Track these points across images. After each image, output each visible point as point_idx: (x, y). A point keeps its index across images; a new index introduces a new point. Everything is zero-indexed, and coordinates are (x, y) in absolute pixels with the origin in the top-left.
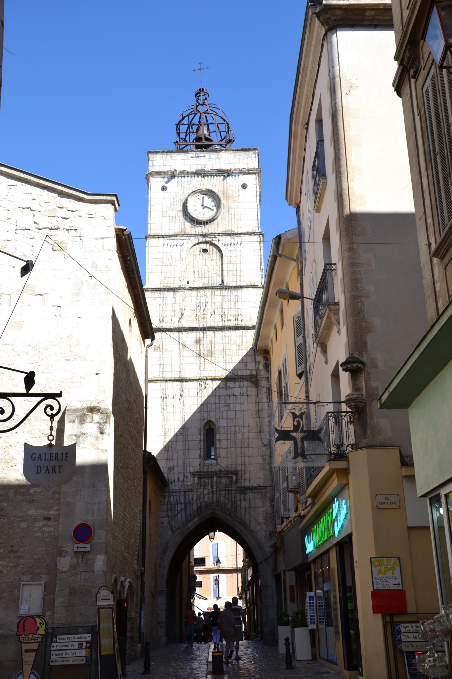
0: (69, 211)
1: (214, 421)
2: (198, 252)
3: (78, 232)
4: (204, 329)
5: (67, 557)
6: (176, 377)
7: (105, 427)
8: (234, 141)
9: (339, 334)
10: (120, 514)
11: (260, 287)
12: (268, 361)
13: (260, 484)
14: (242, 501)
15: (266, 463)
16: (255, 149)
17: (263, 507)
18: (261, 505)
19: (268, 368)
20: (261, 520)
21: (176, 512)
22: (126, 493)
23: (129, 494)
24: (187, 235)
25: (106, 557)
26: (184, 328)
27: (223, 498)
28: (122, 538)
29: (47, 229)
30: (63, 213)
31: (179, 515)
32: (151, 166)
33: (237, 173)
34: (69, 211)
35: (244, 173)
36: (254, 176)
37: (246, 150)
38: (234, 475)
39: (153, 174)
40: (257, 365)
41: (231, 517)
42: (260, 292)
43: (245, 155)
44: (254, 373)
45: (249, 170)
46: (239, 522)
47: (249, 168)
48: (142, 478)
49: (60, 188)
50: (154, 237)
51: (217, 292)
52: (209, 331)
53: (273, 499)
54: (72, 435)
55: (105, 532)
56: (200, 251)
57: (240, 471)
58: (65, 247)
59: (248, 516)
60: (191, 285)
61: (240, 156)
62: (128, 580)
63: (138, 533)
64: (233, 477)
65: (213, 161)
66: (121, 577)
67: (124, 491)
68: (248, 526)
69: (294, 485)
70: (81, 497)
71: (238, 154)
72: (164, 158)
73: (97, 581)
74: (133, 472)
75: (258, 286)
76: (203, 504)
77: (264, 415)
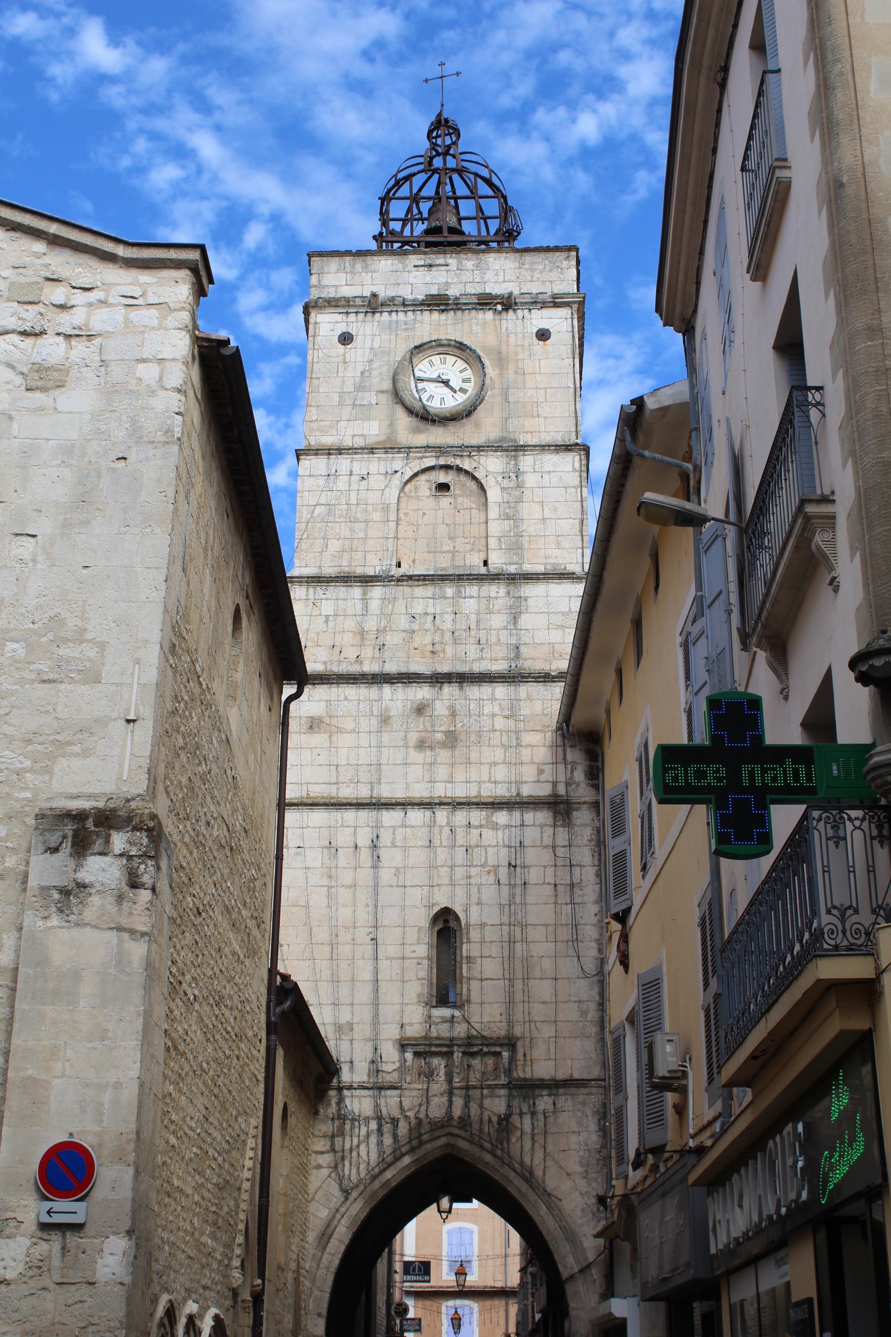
0: (74, 288)
1: (458, 910)
2: (427, 493)
3: (97, 341)
4: (438, 679)
5: (19, 1238)
6: (363, 796)
7: (143, 867)
8: (519, 233)
9: (836, 590)
10: (191, 1129)
11: (578, 578)
12: (596, 760)
13: (572, 1074)
14: (524, 1116)
15: (589, 1019)
16: (569, 249)
17: (579, 1133)
19: (598, 778)
22: (212, 1072)
23: (222, 1077)
24: (399, 450)
25: (133, 1243)
26: (388, 674)
28: (196, 1196)
29: (15, 338)
30: (59, 294)
31: (363, 1148)
32: (315, 286)
33: (526, 303)
34: (74, 288)
35: (544, 303)
36: (565, 312)
38: (506, 1048)
40: (569, 772)
41: (495, 1156)
42: (579, 589)
43: (547, 262)
44: (561, 790)
45: (554, 296)
46: (514, 1170)
47: (556, 291)
48: (264, 1041)
49: (53, 228)
50: (317, 452)
51: (472, 590)
52: (449, 682)
53: (605, 1113)
54: (48, 888)
55: (131, 1170)
56: (430, 489)
58: (60, 381)
59: (539, 1154)
60: (404, 570)
61: (532, 264)
62: (213, 1311)
63: (246, 1185)
64: (504, 1053)
65: (467, 276)
66: (190, 1302)
67: (205, 1065)
68: (540, 1181)
69: (670, 1068)
70: (67, 1065)
71: (528, 258)
72: (348, 269)
73: (105, 1313)
74: (235, 1018)
75: (574, 573)
77: (586, 898)
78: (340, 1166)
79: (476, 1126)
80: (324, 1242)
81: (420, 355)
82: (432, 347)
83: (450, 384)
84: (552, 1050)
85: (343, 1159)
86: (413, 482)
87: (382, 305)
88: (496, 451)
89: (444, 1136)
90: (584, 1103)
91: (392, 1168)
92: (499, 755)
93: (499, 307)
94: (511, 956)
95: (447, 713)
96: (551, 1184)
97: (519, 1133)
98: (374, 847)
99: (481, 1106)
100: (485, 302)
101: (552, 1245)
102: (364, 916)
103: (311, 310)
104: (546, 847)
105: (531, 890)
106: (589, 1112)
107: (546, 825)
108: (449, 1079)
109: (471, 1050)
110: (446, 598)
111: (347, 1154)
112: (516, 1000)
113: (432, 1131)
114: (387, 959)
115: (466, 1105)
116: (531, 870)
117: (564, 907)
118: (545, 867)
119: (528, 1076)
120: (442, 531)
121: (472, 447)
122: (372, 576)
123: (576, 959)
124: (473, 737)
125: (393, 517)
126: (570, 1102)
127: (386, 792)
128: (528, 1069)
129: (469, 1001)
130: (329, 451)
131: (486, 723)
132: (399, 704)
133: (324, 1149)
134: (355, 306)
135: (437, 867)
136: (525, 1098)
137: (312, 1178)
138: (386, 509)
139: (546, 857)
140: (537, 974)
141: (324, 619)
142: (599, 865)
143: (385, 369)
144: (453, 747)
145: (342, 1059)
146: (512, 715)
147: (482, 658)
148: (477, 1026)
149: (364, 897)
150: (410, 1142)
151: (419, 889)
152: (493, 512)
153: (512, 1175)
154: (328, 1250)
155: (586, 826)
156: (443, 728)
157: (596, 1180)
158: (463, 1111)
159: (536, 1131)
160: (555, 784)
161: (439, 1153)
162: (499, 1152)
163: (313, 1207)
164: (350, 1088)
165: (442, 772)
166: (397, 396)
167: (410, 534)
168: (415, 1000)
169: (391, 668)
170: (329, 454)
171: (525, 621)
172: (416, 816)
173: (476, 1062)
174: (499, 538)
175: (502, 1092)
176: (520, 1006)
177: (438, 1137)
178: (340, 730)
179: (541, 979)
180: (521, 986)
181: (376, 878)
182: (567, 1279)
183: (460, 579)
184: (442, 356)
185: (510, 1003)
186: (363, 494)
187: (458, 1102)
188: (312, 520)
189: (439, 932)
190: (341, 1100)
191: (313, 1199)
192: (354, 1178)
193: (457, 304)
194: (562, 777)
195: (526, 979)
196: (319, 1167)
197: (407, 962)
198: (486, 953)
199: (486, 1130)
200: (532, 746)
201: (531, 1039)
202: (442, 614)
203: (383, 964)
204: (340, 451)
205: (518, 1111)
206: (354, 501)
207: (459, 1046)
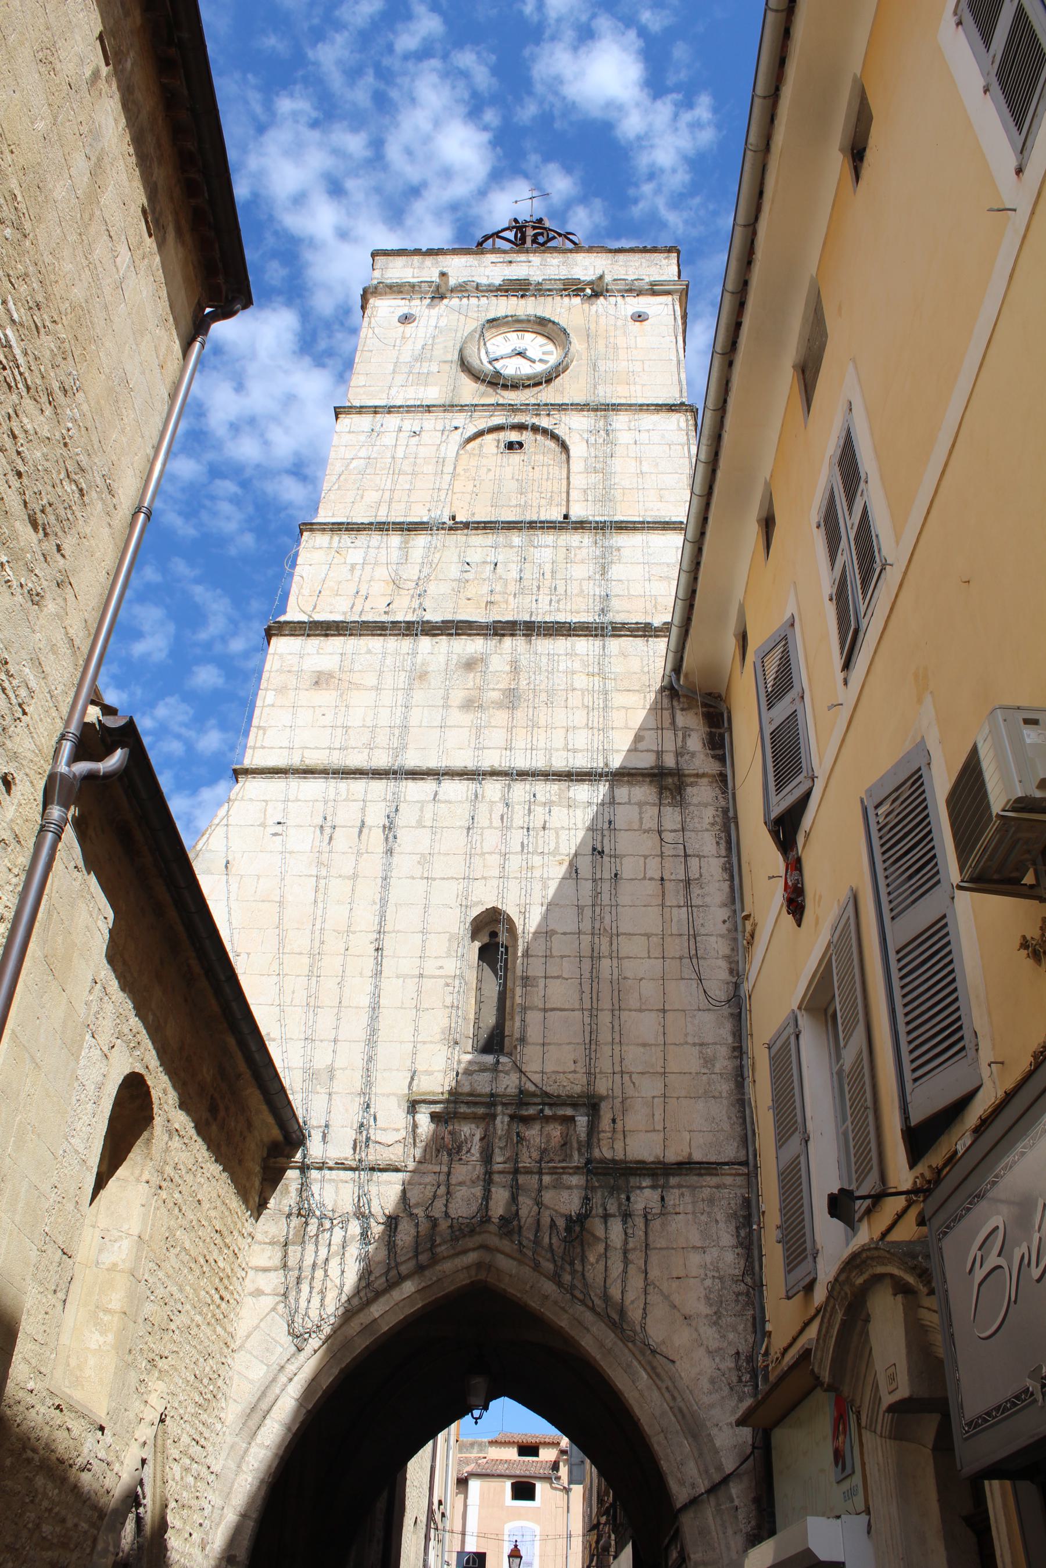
13: (690, 1154)
18: (695, 1239)
19: (722, 746)
20: (694, 1301)
21: (323, 1252)
24: (462, 408)
27: (529, 1202)
33: (619, 291)
37: (645, 250)
38: (583, 1110)
39: (379, 290)
41: (560, 1284)
44: (670, 761)
45: (653, 284)
46: (593, 1309)
50: (361, 410)
51: (548, 538)
52: (512, 635)
57: (607, 1097)
59: (636, 1282)
68: (638, 1328)
76: (444, 1225)
77: (708, 900)
80: (252, 1423)
81: (494, 330)
82: (507, 323)
83: (528, 354)
84: (658, 1117)
86: (479, 441)
87: (452, 291)
88: (582, 410)
89: (473, 1250)
90: (711, 1201)
91: (382, 1300)
92: (579, 718)
93: (589, 291)
94: (595, 977)
95: (508, 668)
96: (656, 1333)
97: (601, 1248)
98: (389, 828)
99: (539, 1203)
100: (572, 288)
101: (658, 1443)
102: (366, 918)
103: (369, 296)
104: (647, 831)
105: (625, 888)
107: (648, 803)
108: (487, 1157)
109: (524, 1113)
110: (512, 547)
111: (307, 1273)
112: (601, 1038)
113: (455, 1239)
114: (398, 977)
115: (514, 1198)
116: (625, 861)
117: (675, 911)
118: (646, 857)
119: (619, 1156)
120: (514, 485)
121: (552, 405)
123: (694, 984)
124: (544, 696)
125: (449, 469)
126: (688, 1198)
127: (412, 760)
128: (619, 1145)
129: (523, 1040)
130: (375, 410)
131: (560, 681)
132: (442, 659)
134: (421, 292)
135: (483, 854)
136: (613, 1190)
137: (244, 1312)
139: (649, 844)
140: (633, 1002)
141: (349, 567)
142: (729, 856)
143: (451, 343)
145: (313, 1122)
146: (602, 674)
147: (558, 610)
148: (536, 1078)
149: (369, 890)
150: (416, 1256)
151: (454, 883)
152: (576, 465)
153: (588, 1317)
154: (259, 1439)
155: (706, 805)
156: (501, 686)
157: (735, 1329)
159: (631, 1245)
160: (659, 754)
161: (463, 1280)
162: (567, 1278)
163: (239, 1362)
164: (321, 1167)
165: (496, 737)
166: (465, 366)
168: (438, 1037)
169: (434, 616)
170: (376, 413)
171: (616, 571)
172: (455, 789)
173: (533, 1133)
174: (585, 491)
175: (575, 1180)
176: (607, 1050)
177: (465, 1252)
178: (358, 687)
179: (640, 1010)
180: (609, 1019)
181: (388, 867)
182: (685, 1507)
183: (532, 528)
184: (520, 333)
185: (591, 1044)
186: (412, 449)
187: (500, 1197)
189: (482, 950)
190: (304, 1186)
192: (314, 1314)
193: (540, 290)
194: (669, 745)
195: (617, 1010)
196: (258, 1293)
197: (428, 984)
198: (553, 971)
199: (546, 1240)
200: (627, 709)
202: (505, 563)
203: (390, 986)
204: (390, 409)
205: (600, 1211)
206: (400, 454)
207: (504, 1104)
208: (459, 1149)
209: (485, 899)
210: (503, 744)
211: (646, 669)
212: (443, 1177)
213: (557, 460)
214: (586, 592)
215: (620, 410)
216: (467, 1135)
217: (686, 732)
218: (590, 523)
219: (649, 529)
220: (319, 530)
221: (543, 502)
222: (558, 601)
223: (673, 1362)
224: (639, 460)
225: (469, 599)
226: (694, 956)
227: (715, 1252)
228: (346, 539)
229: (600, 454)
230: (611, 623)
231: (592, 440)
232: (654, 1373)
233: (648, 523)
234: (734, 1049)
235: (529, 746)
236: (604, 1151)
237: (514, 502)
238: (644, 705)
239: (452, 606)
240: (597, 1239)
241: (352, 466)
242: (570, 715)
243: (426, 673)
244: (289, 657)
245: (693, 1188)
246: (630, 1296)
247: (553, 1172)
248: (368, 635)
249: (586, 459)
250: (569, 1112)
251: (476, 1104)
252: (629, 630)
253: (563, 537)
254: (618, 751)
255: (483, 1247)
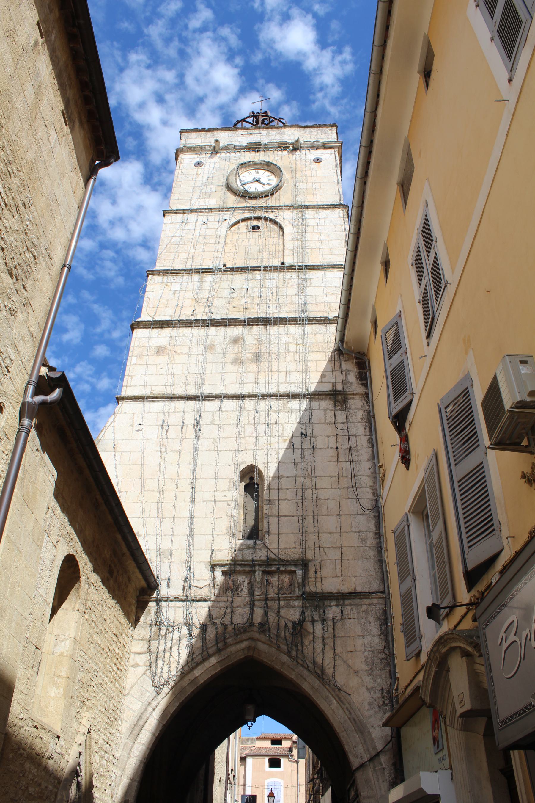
1: (261, 467)
13: (355, 588)
14: (316, 623)
18: (359, 631)
19: (366, 379)
21: (169, 644)
24: (228, 209)
27: (274, 615)
33: (307, 147)
37: (320, 126)
38: (300, 567)
39: (184, 150)
41: (290, 657)
44: (339, 387)
45: (324, 143)
46: (308, 669)
50: (177, 212)
51: (274, 275)
52: (257, 325)
57: (312, 560)
59: (329, 655)
68: (331, 678)
76: (230, 628)
77: (361, 458)
78: (154, 666)
79: (274, 631)
80: (135, 732)
81: (243, 169)
82: (250, 165)
83: (261, 181)
85: (157, 658)
86: (237, 226)
87: (221, 149)
88: (290, 209)
89: (246, 640)
90: (367, 612)
91: (200, 667)
92: (293, 366)
93: (291, 148)
94: (304, 499)
95: (255, 342)
96: (340, 680)
97: (311, 638)
98: (197, 425)
99: (279, 615)
100: (283, 146)
101: (343, 736)
102: (186, 472)
103: (179, 153)
105: (318, 453)
106: (371, 619)
107: (329, 409)
108: (251, 593)
109: (270, 569)
110: (256, 280)
111: (161, 654)
112: (308, 530)
114: (203, 502)
115: (266, 613)
116: (318, 439)
117: (344, 464)
118: (328, 437)
119: (319, 590)
121: (274, 206)
122: (206, 269)
123: (355, 501)
124: (274, 356)
125: (222, 240)
126: (355, 611)
127: (207, 390)
128: (319, 585)
129: (268, 532)
130: (184, 212)
131: (282, 347)
132: (222, 338)
133: (141, 650)
134: (206, 151)
135: (245, 437)
136: (317, 607)
138: (218, 237)
139: (330, 430)
140: (324, 511)
141: (173, 292)
142: (371, 435)
143: (222, 176)
144: (258, 362)
145: (162, 577)
146: (304, 344)
147: (280, 311)
148: (275, 551)
149: (187, 457)
150: (217, 644)
151: (231, 453)
152: (287, 237)
153: (306, 673)
154: (139, 740)
155: (358, 409)
156: (252, 351)
157: (380, 677)
158: (263, 619)
159: (326, 636)
160: (334, 384)
161: (241, 656)
162: (294, 653)
163: (127, 701)
164: (167, 600)
165: (250, 377)
166: (229, 188)
167: (233, 250)
168: (225, 532)
169: (217, 316)
170: (184, 213)
171: (309, 291)
172: (230, 405)
173: (274, 580)
174: (292, 250)
175: (297, 603)
176: (311, 536)
177: (241, 641)
178: (179, 354)
179: (328, 515)
180: (312, 520)
181: (196, 446)
182: (358, 769)
183: (266, 270)
184: (257, 170)
185: (303, 533)
187: (259, 612)
188: (170, 244)
189: (246, 487)
190: (158, 610)
191: (128, 693)
192: (165, 675)
193: (266, 148)
194: (339, 379)
195: (316, 515)
196: (136, 665)
197: (218, 505)
198: (282, 496)
199: (283, 634)
201: (321, 561)
202: (253, 288)
204: (191, 211)
205: (310, 618)
206: (197, 233)
207: (259, 565)
208: (237, 589)
209: (247, 460)
210: (254, 381)
211: (326, 341)
212: (229, 604)
213: (278, 235)
214: (294, 302)
215: (309, 208)
216: (241, 581)
217: (347, 372)
218: (295, 266)
219: (326, 268)
220: (157, 274)
221: (271, 256)
222: (280, 307)
223: (349, 695)
224: (319, 233)
225: (234, 307)
226: (355, 487)
227: (369, 638)
228: (171, 278)
229: (299, 231)
230: (308, 317)
231: (295, 224)
232: (340, 701)
233: (325, 265)
234: (376, 534)
235: (267, 382)
236: (311, 588)
237: (256, 257)
238: (326, 359)
239: (226, 311)
240: (309, 633)
241: (173, 241)
242: (288, 365)
243: (214, 345)
244: (143, 339)
245: (357, 605)
246: (327, 661)
247: (285, 599)
248: (183, 327)
249: (292, 234)
250: (293, 568)
251: (245, 565)
252: (316, 321)
253: (282, 274)
254: (313, 383)
255: (251, 639)
